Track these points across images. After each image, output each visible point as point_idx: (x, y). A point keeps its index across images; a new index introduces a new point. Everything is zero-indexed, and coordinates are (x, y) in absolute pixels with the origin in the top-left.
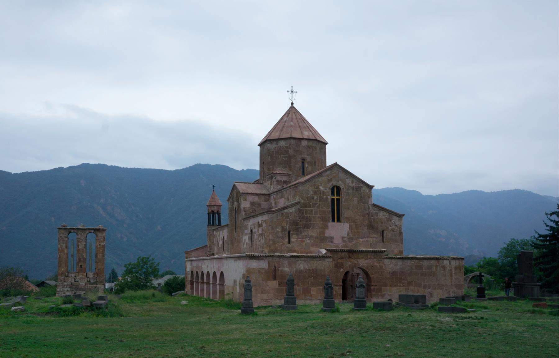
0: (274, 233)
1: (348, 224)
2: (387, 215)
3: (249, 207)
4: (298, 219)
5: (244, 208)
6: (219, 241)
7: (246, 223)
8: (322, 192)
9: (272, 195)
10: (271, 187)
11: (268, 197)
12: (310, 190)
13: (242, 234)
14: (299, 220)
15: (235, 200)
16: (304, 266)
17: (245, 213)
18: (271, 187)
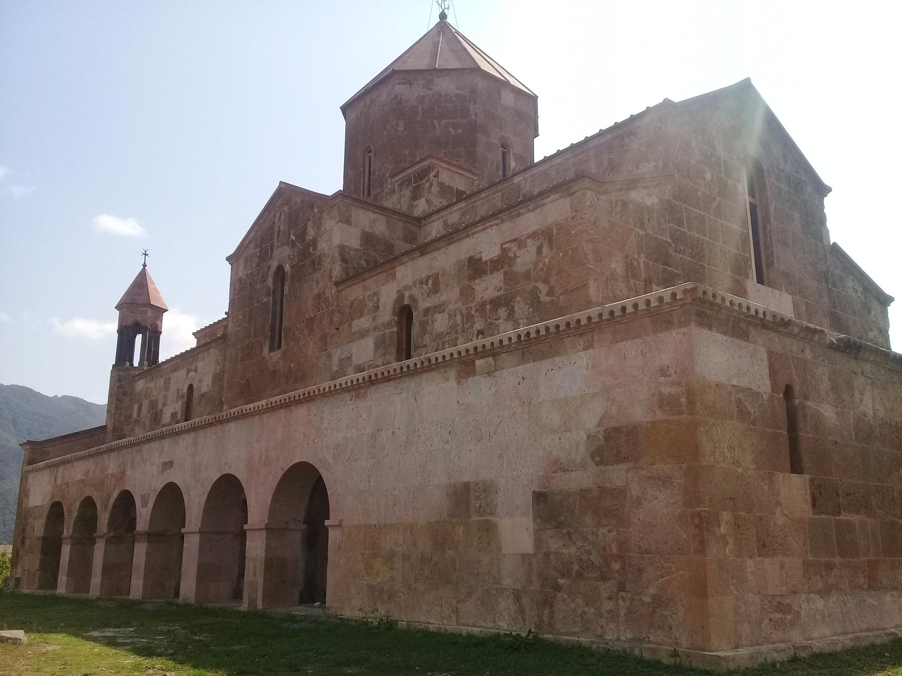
0: (604, 277)
1: (790, 297)
2: (860, 292)
3: (359, 248)
4: (669, 240)
5: (342, 249)
6: (164, 405)
7: (355, 292)
8: (722, 162)
9: (435, 217)
10: (416, 206)
11: (414, 229)
12: (694, 144)
13: (325, 344)
14: (673, 246)
15: (276, 243)
16: (873, 407)
17: (344, 265)
18: (411, 207)
